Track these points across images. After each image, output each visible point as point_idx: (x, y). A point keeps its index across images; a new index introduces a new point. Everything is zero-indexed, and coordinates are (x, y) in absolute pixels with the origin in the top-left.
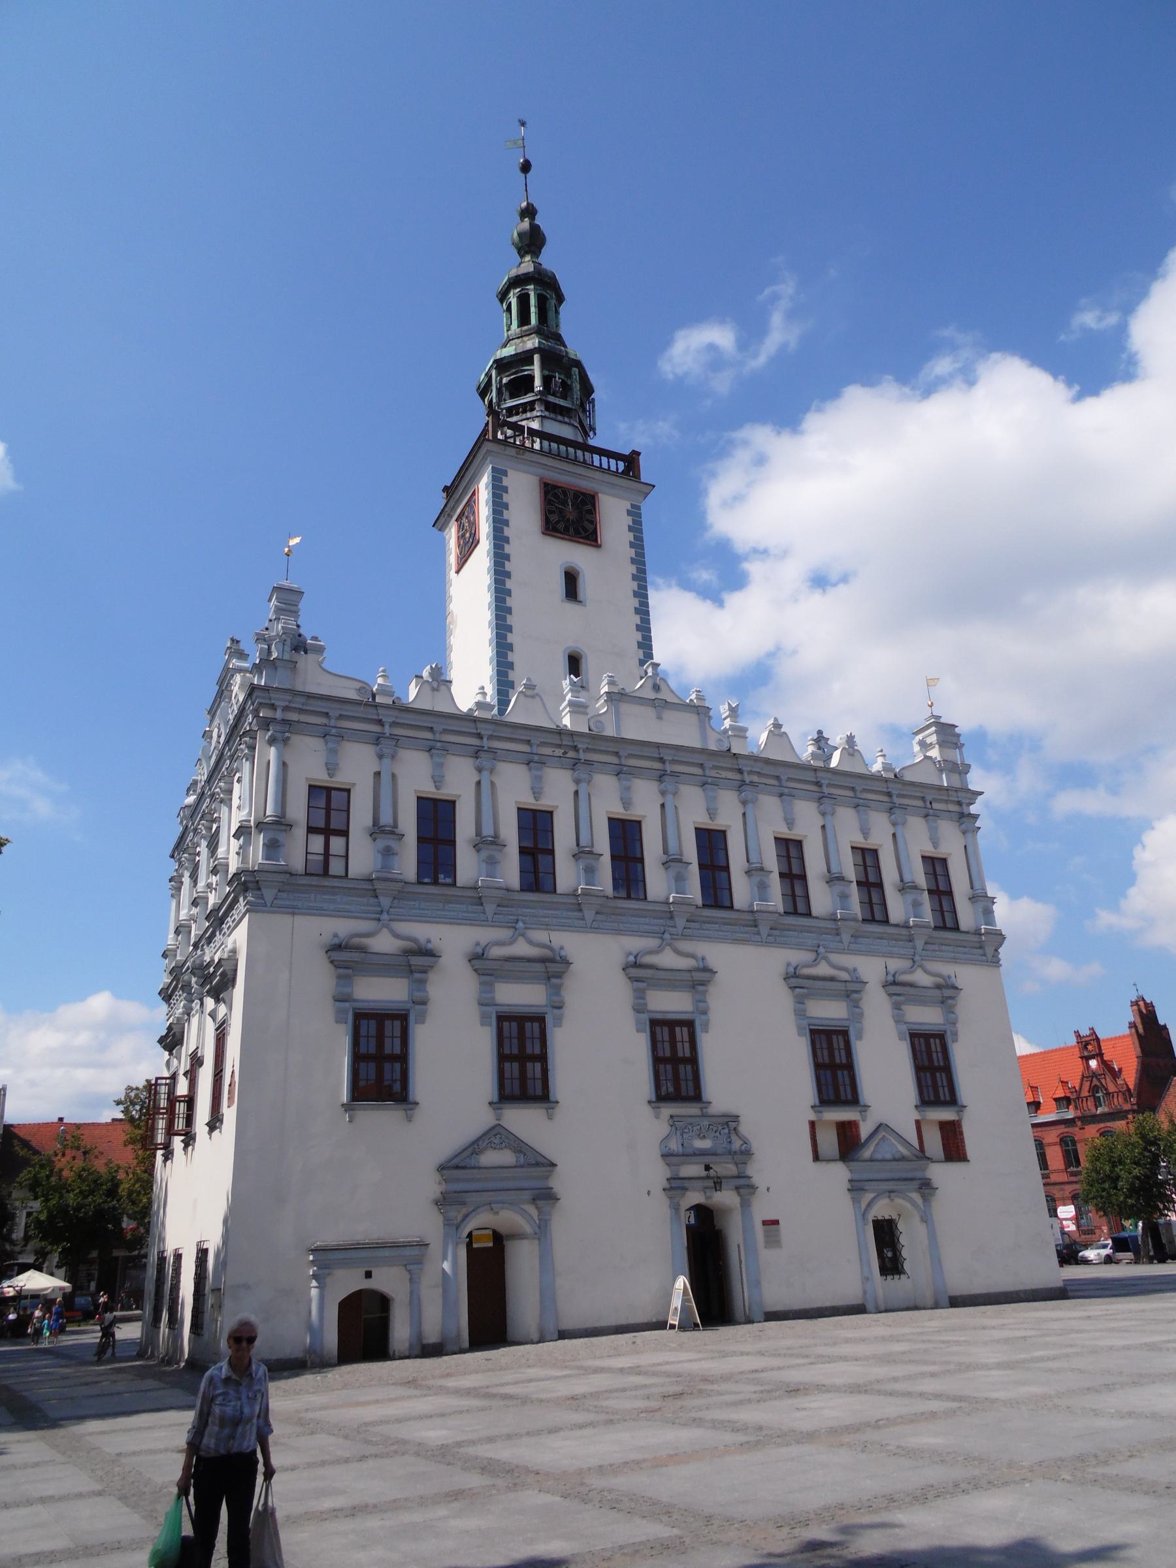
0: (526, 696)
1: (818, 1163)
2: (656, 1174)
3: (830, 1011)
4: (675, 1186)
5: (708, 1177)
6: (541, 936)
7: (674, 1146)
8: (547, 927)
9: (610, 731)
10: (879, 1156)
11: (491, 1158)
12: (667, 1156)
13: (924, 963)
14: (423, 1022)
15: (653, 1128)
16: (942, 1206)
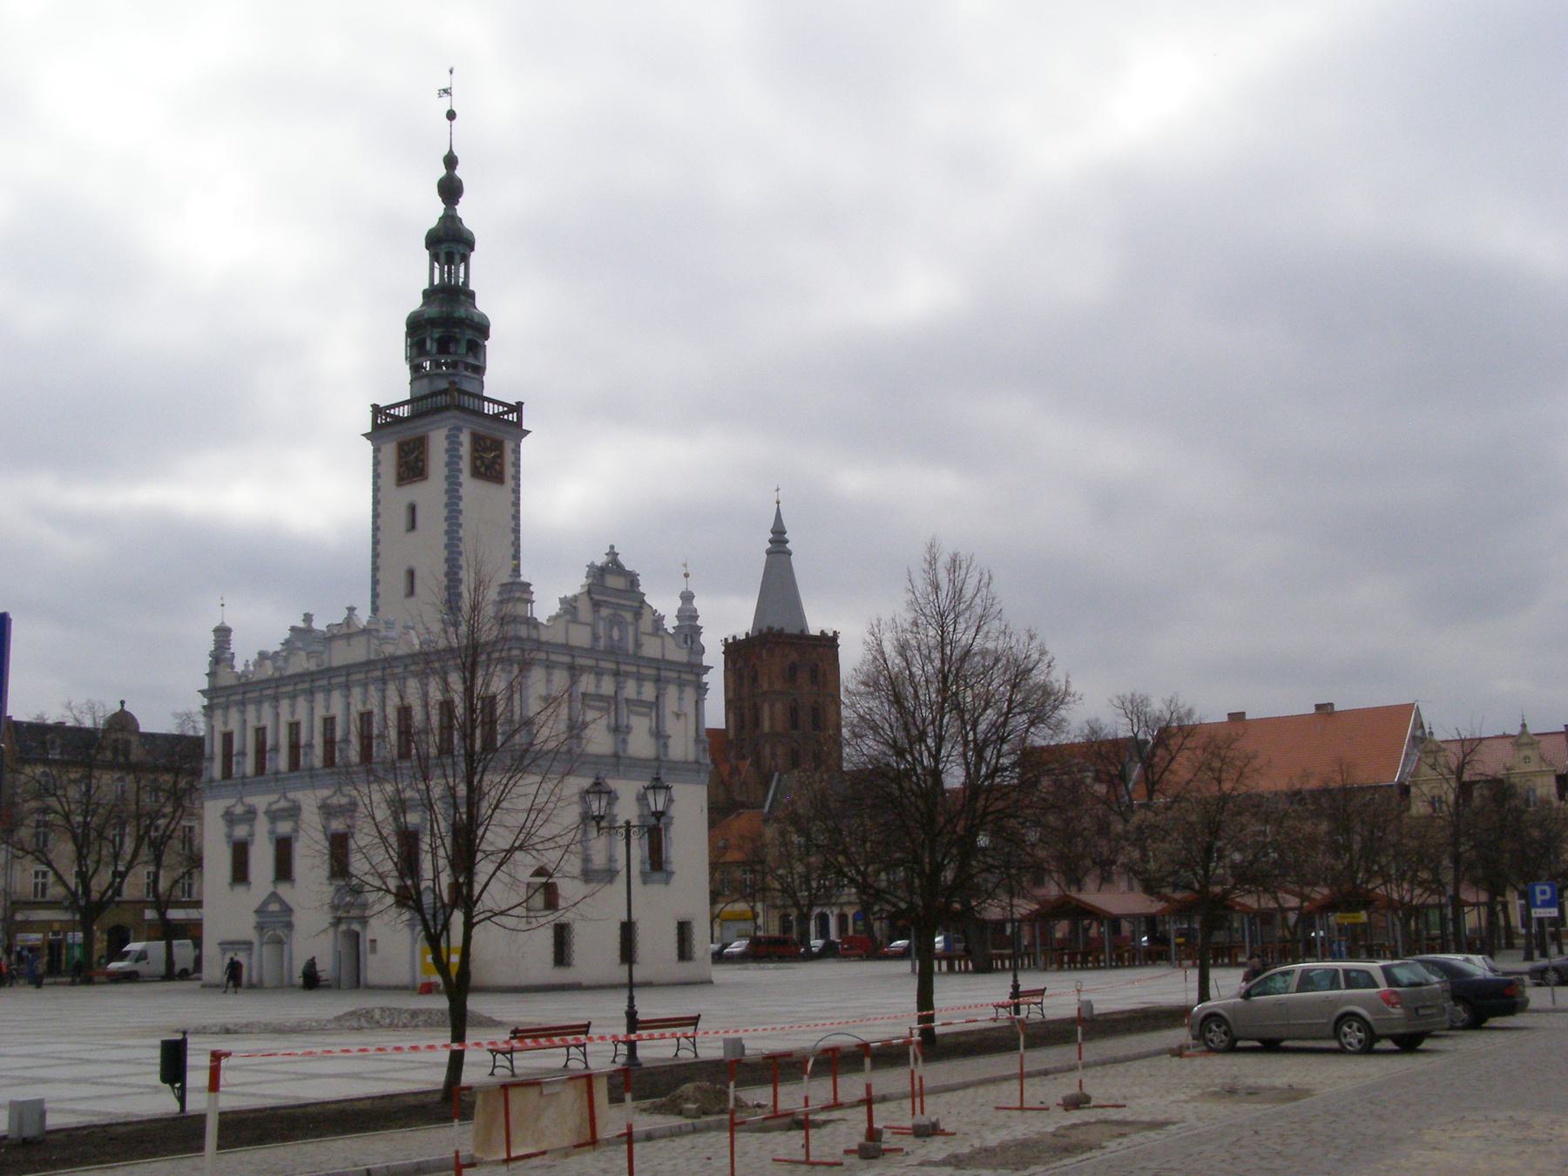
6: (291, 795)
12: (335, 908)
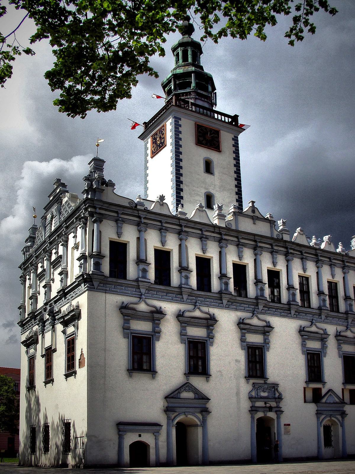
0: (200, 211)
1: (306, 404)
2: (246, 404)
3: (314, 345)
4: (253, 410)
5: (266, 407)
6: (205, 309)
7: (253, 394)
8: (208, 306)
9: (234, 227)
10: (328, 401)
11: (185, 395)
12: (251, 398)
13: (351, 328)
14: (158, 340)
15: (245, 388)
16: (348, 421)
